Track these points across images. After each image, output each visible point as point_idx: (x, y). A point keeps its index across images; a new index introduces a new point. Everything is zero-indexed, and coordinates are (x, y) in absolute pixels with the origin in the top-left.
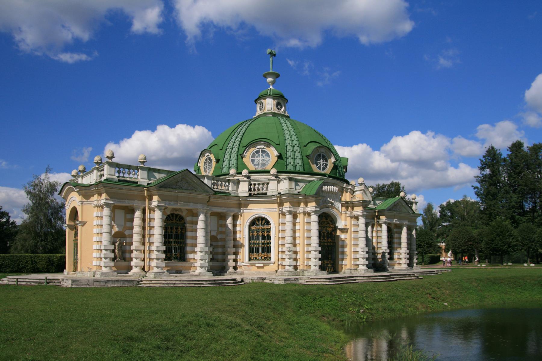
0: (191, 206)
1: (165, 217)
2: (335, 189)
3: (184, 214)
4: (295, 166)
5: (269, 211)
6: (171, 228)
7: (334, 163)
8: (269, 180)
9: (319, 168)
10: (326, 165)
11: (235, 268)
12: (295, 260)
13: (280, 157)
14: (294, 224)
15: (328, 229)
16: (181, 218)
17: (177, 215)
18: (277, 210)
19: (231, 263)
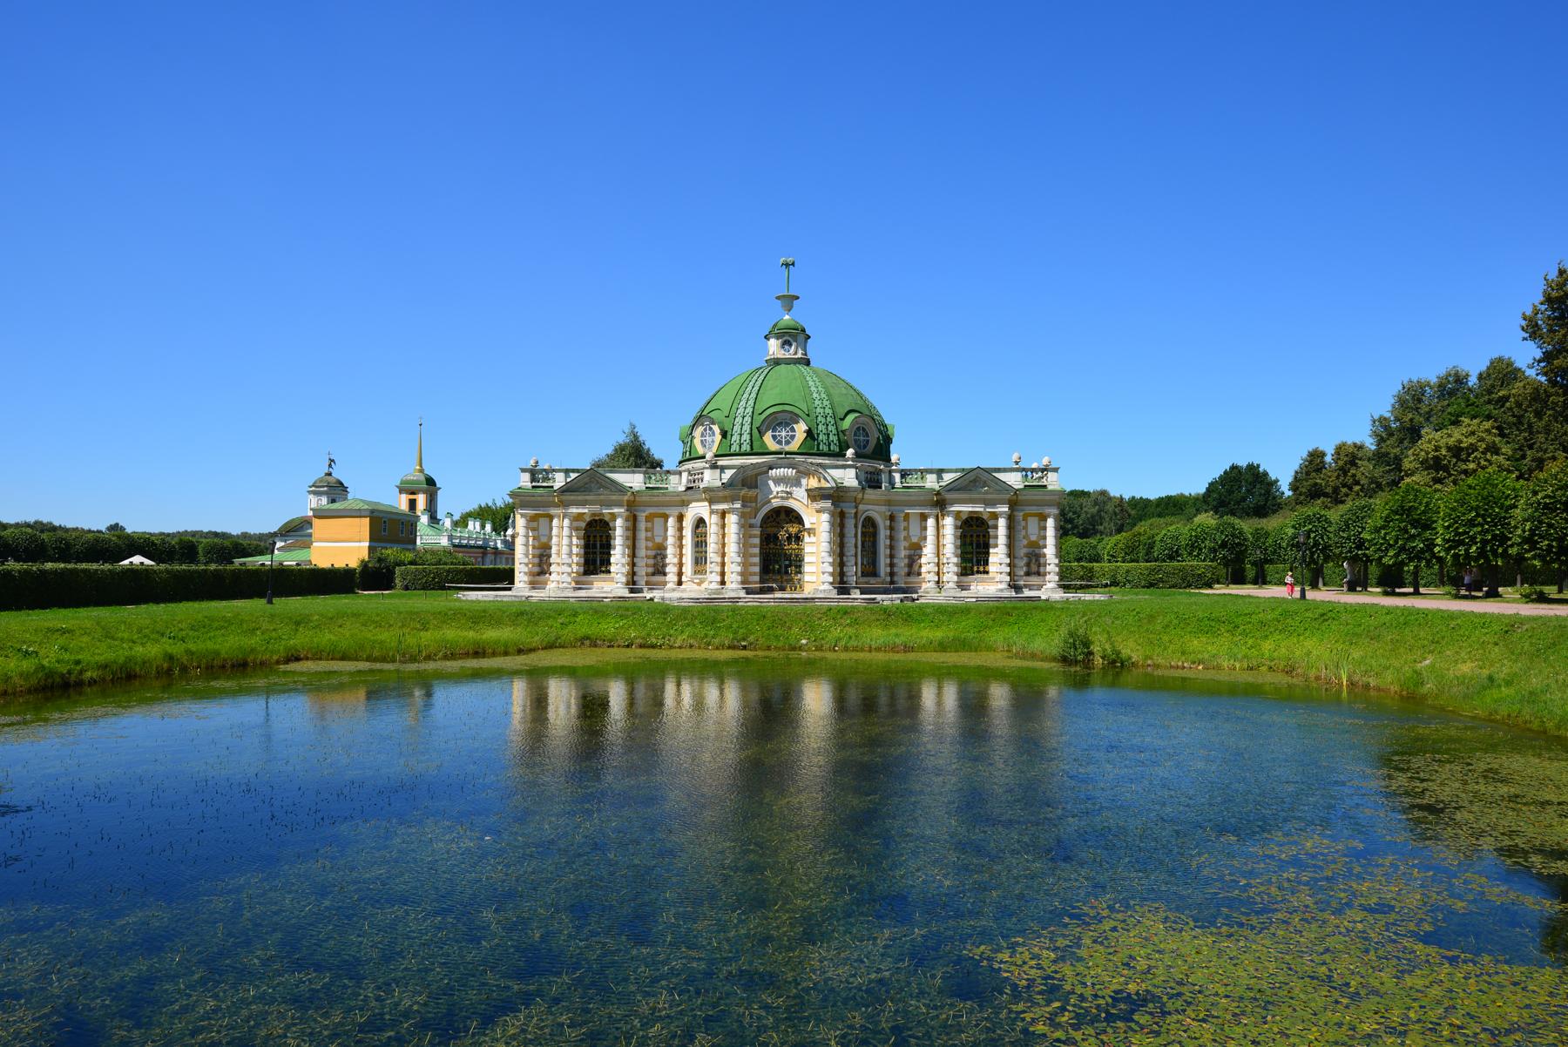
1: (583, 525)
2: (791, 472)
7: (809, 433)
9: (780, 442)
10: (793, 437)
11: (680, 583)
12: (723, 574)
13: (724, 434)
14: (723, 526)
19: (671, 577)
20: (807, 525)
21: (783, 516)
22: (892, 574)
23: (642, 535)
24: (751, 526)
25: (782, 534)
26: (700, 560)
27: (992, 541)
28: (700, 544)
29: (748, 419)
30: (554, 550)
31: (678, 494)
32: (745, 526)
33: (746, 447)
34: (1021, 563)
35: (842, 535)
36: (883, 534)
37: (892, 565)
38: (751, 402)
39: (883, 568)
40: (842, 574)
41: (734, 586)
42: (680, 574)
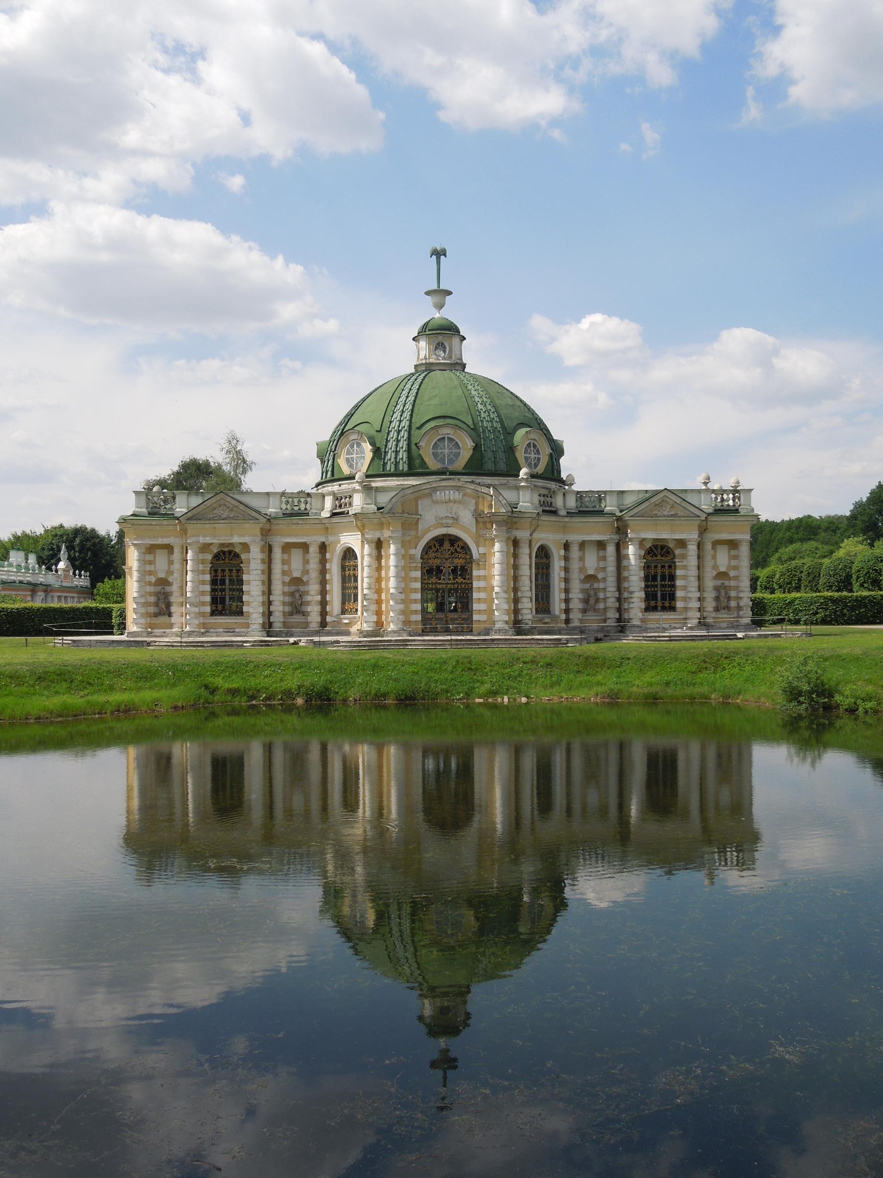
0: (242, 540)
1: (209, 557)
3: (237, 550)
4: (397, 464)
5: (351, 539)
6: (223, 571)
8: (355, 491)
9: (442, 461)
10: (457, 455)
12: (379, 613)
15: (456, 561)
16: (237, 556)
17: (230, 552)
18: (360, 537)
20: (475, 555)
21: (447, 545)
22: (567, 611)
23: (277, 568)
24: (412, 557)
25: (447, 566)
26: (349, 596)
27: (679, 573)
28: (349, 578)
29: (404, 434)
30: (175, 588)
31: (321, 521)
32: (404, 557)
33: (403, 467)
34: (710, 595)
35: (516, 567)
36: (557, 564)
37: (567, 601)
38: (407, 415)
39: (557, 606)
40: (516, 611)
41: (392, 627)
42: (324, 613)
